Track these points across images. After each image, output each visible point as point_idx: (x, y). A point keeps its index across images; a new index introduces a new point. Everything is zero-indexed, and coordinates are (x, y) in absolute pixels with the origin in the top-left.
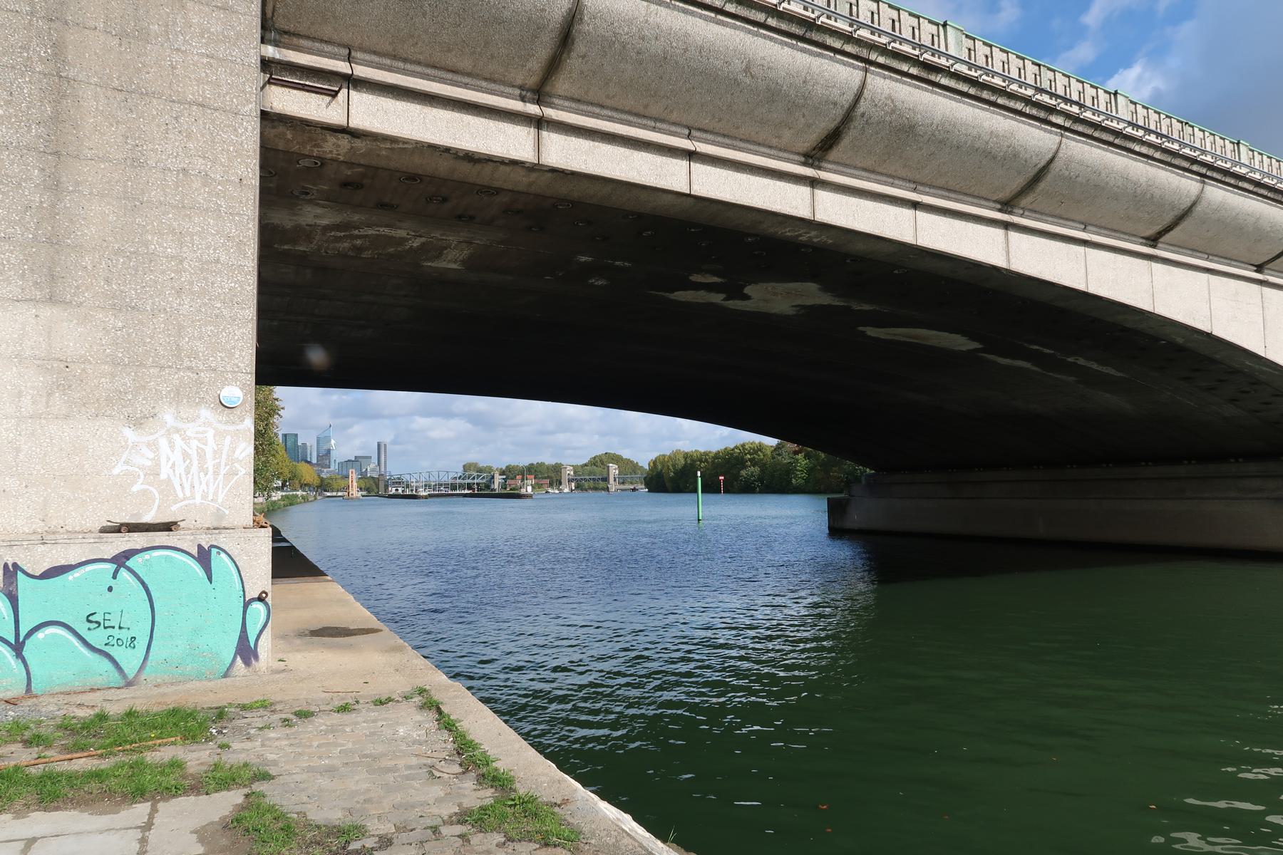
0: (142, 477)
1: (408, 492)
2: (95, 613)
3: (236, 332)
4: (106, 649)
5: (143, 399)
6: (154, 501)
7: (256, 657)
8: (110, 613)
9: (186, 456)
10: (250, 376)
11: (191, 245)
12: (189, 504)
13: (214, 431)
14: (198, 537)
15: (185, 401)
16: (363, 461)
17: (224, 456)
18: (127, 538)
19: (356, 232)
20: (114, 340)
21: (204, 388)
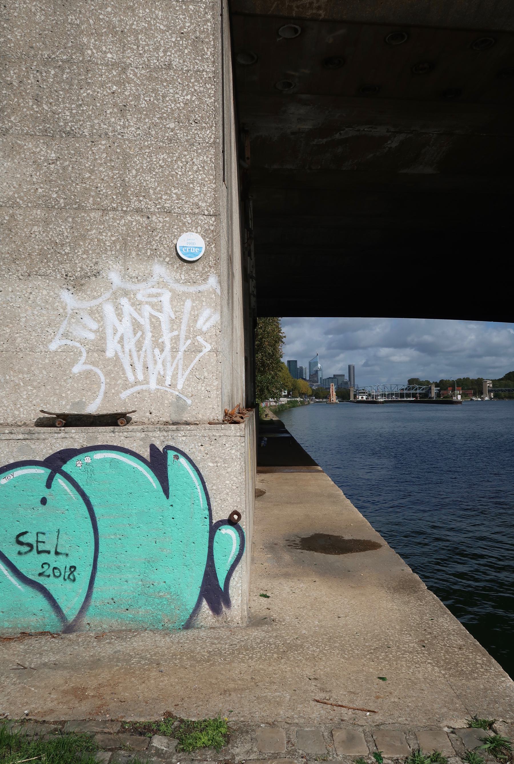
0: (84, 354)
1: (370, 399)
2: (26, 533)
3: (194, 160)
4: (41, 580)
5: (84, 253)
6: (99, 387)
7: (228, 603)
8: (44, 534)
9: (137, 326)
10: (213, 219)
11: (135, 47)
12: (142, 390)
13: (170, 294)
14: (151, 434)
15: (134, 254)
16: (339, 378)
17: (184, 327)
18: (62, 435)
19: (337, 136)
20: (46, 176)
21: (156, 236)
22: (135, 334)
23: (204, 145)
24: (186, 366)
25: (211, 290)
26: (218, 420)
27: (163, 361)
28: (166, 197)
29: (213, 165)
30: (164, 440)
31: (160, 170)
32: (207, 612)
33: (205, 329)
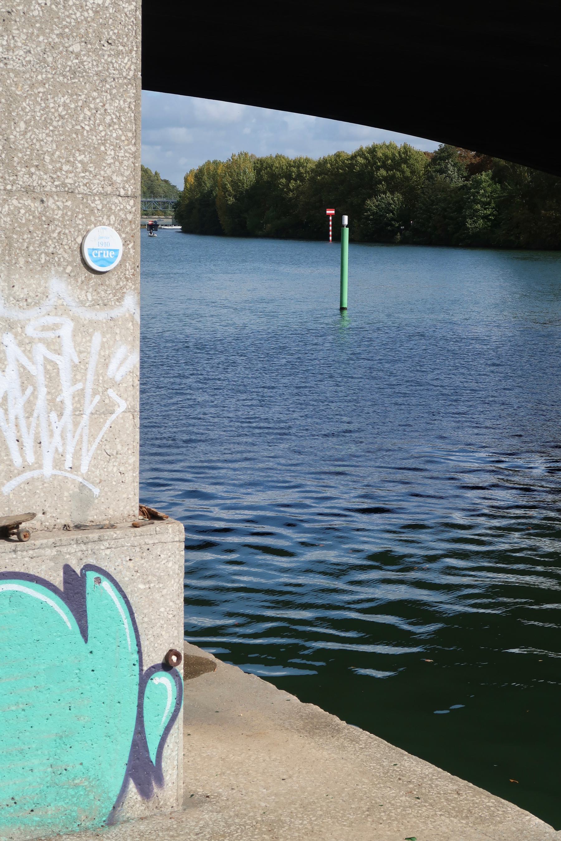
3: (107, 106)
7: (160, 780)
10: (132, 202)
14: (64, 550)
15: (22, 261)
17: (90, 376)
21: (54, 231)
22: (23, 390)
23: (120, 81)
24: (93, 436)
25: (127, 316)
26: (134, 516)
27: (62, 432)
28: (68, 167)
29: (133, 115)
30: (82, 556)
31: (60, 123)
32: (134, 798)
33: (118, 378)
